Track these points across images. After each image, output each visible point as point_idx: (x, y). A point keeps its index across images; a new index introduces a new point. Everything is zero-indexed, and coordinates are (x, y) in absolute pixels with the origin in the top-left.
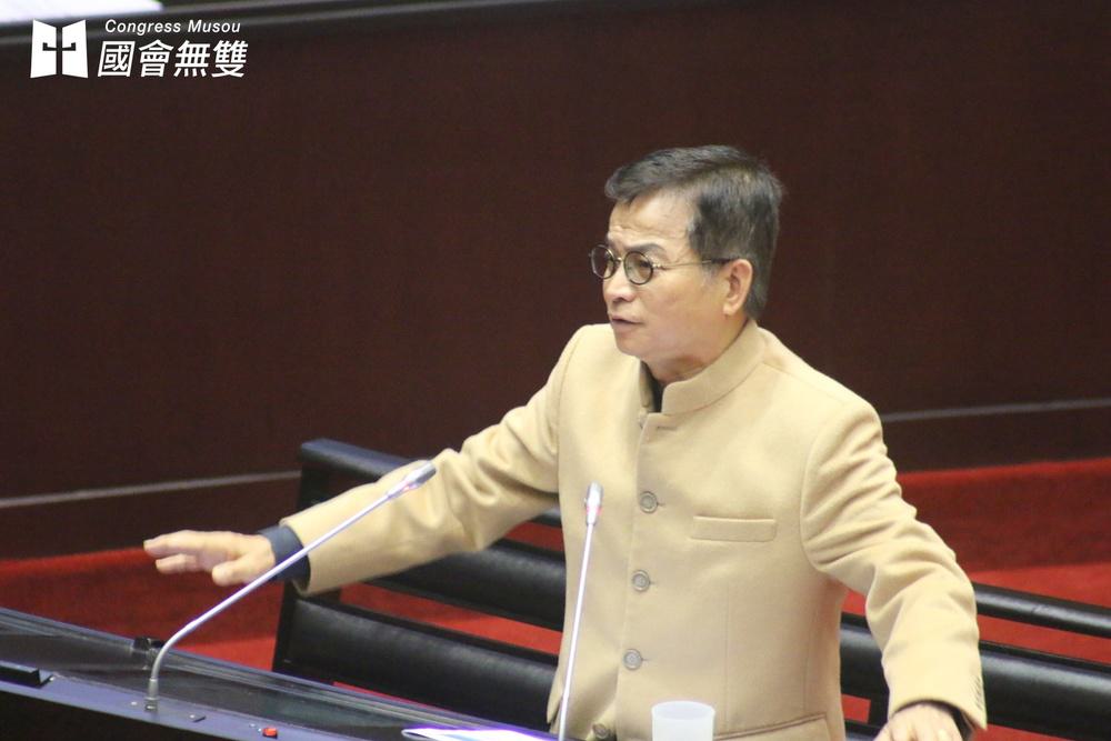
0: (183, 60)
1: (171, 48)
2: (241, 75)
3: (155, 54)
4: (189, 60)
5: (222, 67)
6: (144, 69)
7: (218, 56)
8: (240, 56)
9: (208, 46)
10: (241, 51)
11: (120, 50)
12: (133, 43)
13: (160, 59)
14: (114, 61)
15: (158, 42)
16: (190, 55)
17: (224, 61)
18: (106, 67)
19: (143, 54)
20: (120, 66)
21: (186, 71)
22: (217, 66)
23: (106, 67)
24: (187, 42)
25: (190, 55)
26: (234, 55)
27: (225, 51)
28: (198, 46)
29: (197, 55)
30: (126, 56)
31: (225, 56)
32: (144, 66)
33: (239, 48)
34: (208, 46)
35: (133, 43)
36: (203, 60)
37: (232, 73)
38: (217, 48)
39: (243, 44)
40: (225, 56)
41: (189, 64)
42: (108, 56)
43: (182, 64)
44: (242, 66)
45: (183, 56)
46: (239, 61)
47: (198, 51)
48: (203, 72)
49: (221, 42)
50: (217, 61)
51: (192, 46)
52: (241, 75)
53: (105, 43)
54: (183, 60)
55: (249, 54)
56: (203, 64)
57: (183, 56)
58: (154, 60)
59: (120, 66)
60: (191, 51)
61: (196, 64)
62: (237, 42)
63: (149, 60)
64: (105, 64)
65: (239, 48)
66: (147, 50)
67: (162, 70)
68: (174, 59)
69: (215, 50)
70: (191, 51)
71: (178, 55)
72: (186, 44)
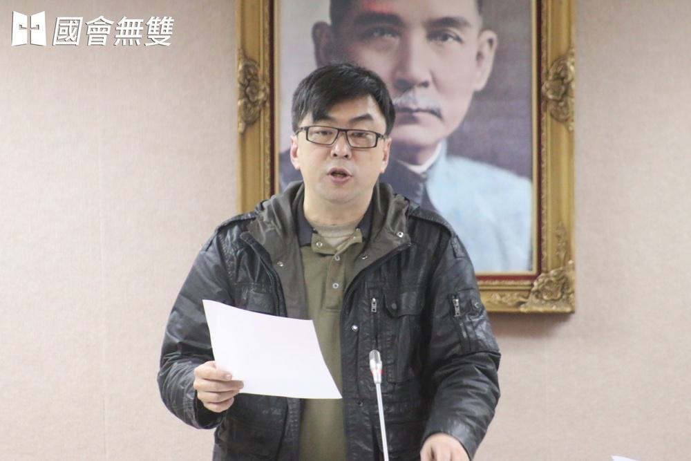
0: (122, 32)
1: (111, 23)
2: (168, 44)
3: (99, 27)
4: (127, 32)
5: (153, 37)
6: (91, 39)
7: (150, 29)
8: (168, 29)
9: (142, 21)
10: (168, 24)
11: (71, 24)
12: (81, 19)
13: (103, 32)
14: (66, 33)
15: (102, 17)
16: (128, 28)
17: (155, 33)
18: (60, 38)
19: (90, 27)
20: (71, 36)
21: (124, 40)
22: (150, 37)
23: (60, 38)
24: (125, 18)
25: (128, 28)
26: (163, 28)
27: (156, 25)
28: (134, 21)
29: (133, 28)
30: (76, 29)
31: (155, 29)
32: (91, 36)
33: (167, 22)
34: (142, 21)
35: (81, 19)
36: (138, 32)
37: (161, 42)
38: (150, 23)
39: (170, 19)
40: (155, 29)
41: (127, 35)
42: (61, 28)
43: (122, 35)
44: (167, 38)
45: (122, 29)
46: (167, 33)
47: (134, 24)
48: (138, 41)
49: (152, 17)
50: (150, 33)
51: (129, 21)
52: (168, 44)
53: (59, 19)
54: (122, 32)
55: (175, 28)
56: (138, 35)
57: (122, 29)
58: (99, 32)
59: (71, 36)
60: (128, 24)
61: (132, 35)
62: (165, 18)
63: (94, 32)
64: (59, 34)
65: (167, 22)
66: (94, 24)
67: (105, 40)
68: (115, 31)
69: (148, 24)
70: (128, 24)
71: (118, 28)
72: (124, 20)
